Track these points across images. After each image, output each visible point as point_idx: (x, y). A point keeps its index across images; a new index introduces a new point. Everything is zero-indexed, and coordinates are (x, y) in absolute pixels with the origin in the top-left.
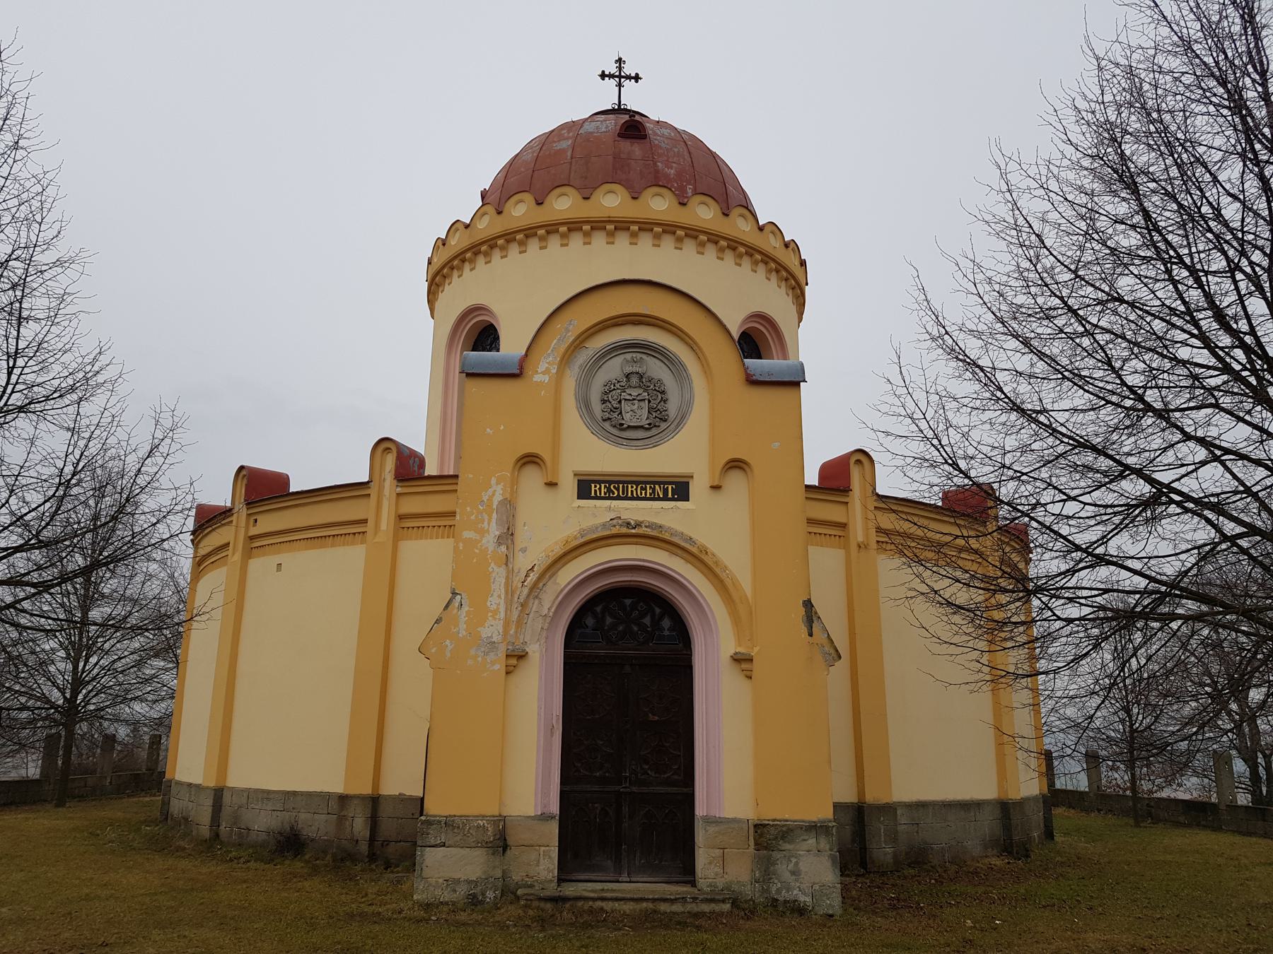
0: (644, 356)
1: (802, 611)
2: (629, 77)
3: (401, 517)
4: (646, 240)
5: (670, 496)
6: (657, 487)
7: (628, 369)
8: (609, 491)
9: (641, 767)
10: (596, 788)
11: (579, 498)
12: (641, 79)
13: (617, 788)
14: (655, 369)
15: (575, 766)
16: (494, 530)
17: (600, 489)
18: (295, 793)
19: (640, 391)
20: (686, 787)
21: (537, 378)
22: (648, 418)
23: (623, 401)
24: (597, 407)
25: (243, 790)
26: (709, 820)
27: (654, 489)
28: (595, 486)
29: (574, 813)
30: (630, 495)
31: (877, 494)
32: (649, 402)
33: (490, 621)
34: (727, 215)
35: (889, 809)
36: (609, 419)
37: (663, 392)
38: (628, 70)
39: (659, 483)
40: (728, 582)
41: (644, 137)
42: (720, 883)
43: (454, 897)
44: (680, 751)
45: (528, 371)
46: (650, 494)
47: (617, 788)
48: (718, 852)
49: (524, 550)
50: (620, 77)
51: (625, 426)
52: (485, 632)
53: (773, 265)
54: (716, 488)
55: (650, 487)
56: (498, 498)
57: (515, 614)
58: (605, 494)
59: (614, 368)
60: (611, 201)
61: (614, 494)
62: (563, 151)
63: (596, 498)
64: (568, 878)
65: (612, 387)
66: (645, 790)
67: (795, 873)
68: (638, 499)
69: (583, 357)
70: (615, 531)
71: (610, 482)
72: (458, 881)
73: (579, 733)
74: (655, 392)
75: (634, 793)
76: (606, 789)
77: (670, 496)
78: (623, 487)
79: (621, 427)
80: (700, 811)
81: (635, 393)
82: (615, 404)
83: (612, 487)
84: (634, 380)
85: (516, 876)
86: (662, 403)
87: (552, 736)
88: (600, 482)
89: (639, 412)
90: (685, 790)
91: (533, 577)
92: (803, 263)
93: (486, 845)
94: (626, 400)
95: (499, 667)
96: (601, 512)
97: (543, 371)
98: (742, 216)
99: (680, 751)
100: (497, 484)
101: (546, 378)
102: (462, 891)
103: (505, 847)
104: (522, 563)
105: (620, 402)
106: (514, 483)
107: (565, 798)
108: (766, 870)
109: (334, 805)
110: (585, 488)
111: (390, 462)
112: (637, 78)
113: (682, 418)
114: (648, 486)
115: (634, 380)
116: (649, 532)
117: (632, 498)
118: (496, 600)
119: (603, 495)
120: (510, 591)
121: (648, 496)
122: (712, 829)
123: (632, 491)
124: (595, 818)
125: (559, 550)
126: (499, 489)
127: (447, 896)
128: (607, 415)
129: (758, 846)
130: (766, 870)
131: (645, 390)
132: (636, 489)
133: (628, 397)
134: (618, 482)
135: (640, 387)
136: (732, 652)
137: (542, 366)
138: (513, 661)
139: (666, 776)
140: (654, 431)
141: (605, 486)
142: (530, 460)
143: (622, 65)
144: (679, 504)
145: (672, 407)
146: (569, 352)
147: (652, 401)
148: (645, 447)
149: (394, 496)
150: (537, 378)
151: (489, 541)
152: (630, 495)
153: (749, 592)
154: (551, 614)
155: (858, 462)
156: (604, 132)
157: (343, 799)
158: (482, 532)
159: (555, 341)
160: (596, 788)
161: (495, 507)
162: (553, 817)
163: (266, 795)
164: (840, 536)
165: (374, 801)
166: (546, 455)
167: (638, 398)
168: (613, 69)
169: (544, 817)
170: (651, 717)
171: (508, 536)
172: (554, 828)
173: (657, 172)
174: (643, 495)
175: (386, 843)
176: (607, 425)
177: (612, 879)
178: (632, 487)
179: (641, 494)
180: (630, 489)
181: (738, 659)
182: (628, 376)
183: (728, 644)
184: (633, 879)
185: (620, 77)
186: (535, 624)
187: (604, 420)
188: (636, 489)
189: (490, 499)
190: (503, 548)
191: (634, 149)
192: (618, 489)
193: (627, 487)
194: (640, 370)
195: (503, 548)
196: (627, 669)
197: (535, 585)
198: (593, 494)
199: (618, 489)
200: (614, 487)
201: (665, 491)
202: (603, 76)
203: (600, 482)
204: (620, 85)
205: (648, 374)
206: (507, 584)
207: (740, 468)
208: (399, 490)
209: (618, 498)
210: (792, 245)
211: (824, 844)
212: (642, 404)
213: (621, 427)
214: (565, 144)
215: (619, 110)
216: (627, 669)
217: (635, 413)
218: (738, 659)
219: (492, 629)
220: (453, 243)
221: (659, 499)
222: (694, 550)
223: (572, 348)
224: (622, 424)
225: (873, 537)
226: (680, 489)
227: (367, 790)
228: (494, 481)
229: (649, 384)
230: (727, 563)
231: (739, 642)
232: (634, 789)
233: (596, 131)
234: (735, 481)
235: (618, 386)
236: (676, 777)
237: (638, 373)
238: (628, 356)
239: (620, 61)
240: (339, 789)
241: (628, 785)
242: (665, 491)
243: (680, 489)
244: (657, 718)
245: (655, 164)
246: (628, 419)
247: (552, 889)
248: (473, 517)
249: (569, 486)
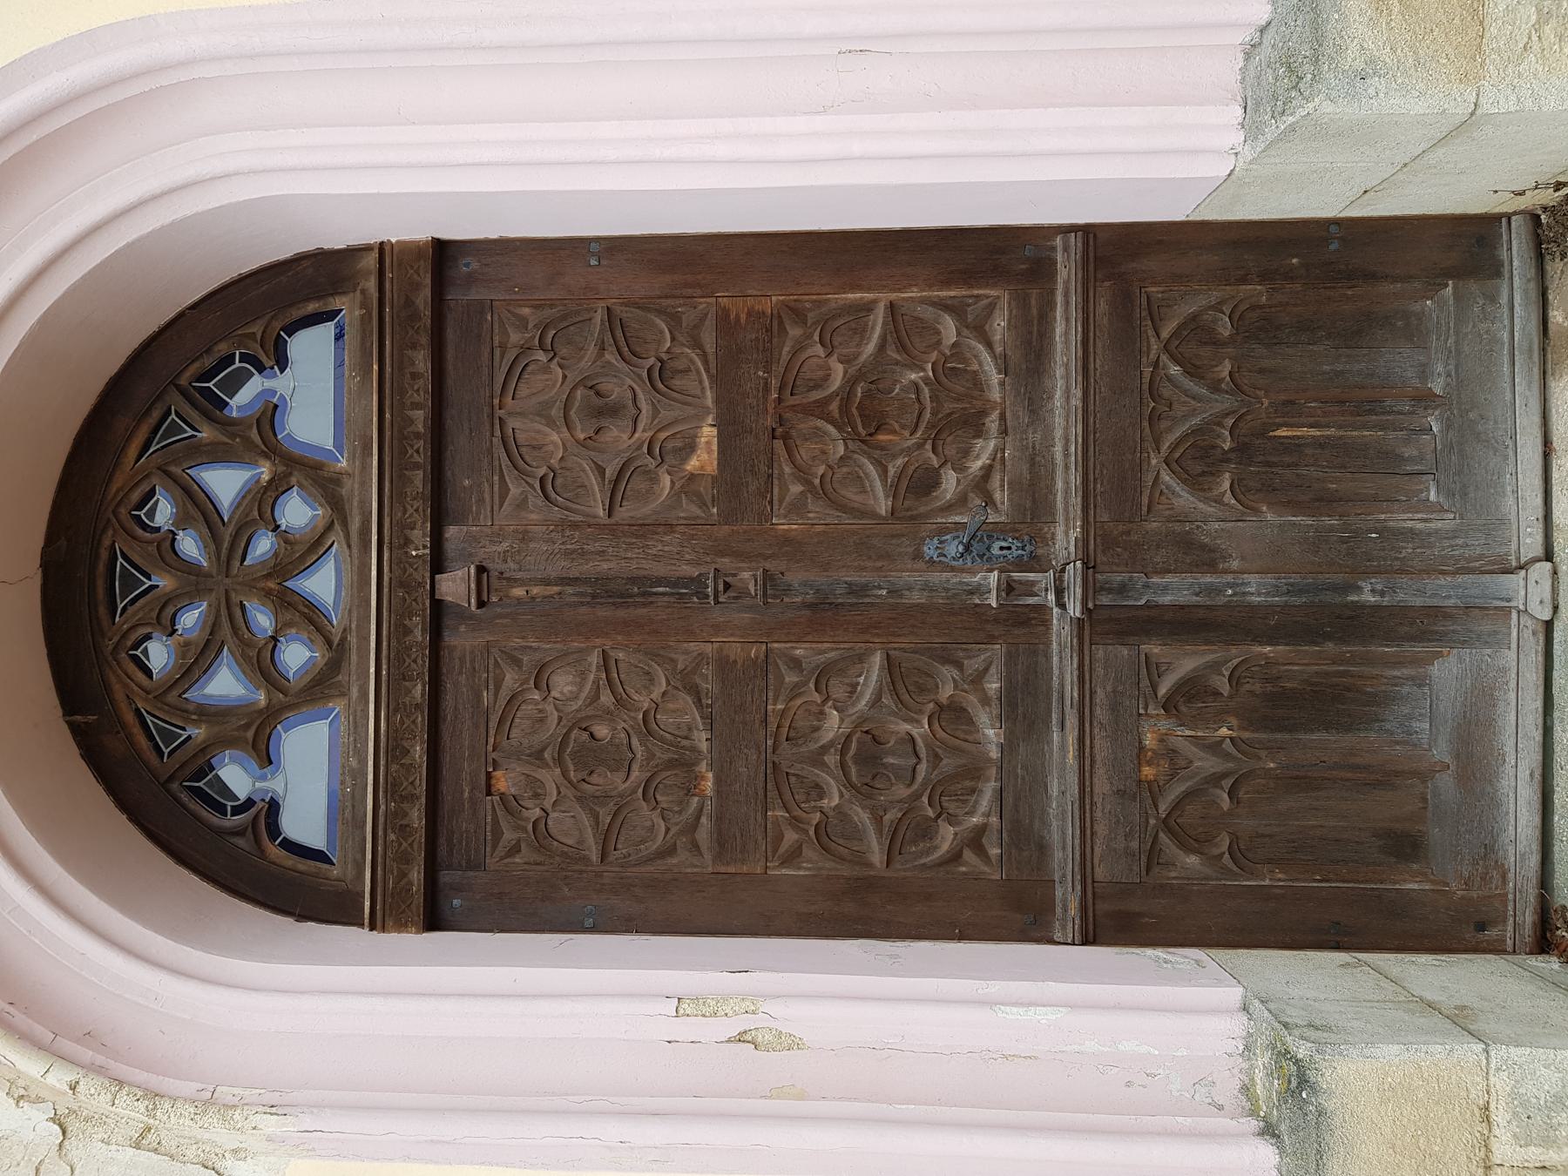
9: (949, 508)
10: (1062, 743)
13: (1060, 631)
15: (955, 857)
20: (1052, 275)
29: (1192, 860)
44: (868, 308)
47: (1060, 631)
64: (1532, 893)
66: (1066, 484)
73: (791, 836)
75: (1084, 542)
76: (1071, 692)
87: (794, 1044)
90: (1066, 271)
99: (868, 308)
124: (1215, 747)
139: (995, 377)
154: (59, 1078)
160: (1062, 743)
170: (704, 458)
177: (1534, 658)
184: (1532, 543)
196: (455, 586)
216: (455, 586)
232: (1065, 539)
236: (999, 325)
241: (1045, 579)
244: (708, 433)
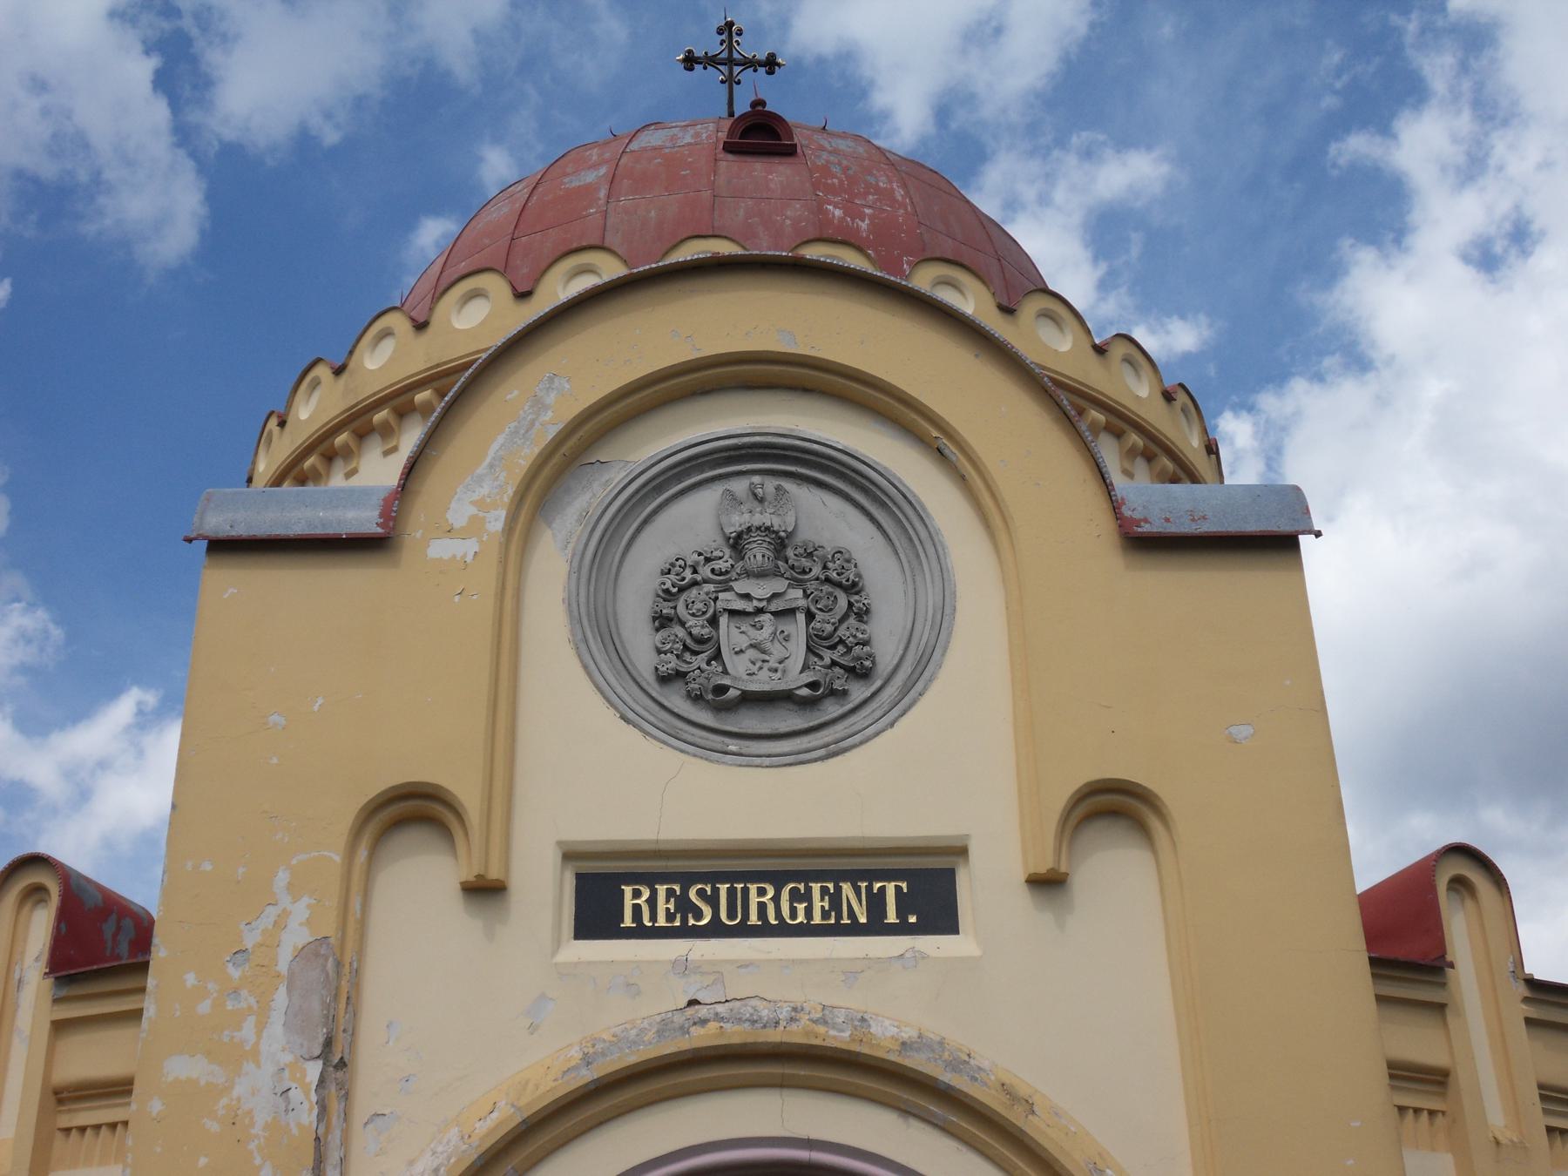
0: (788, 485)
5: (892, 918)
6: (846, 888)
7: (737, 521)
8: (684, 906)
12: (779, 65)
17: (652, 902)
19: (779, 585)
21: (441, 549)
22: (805, 667)
23: (724, 620)
24: (642, 644)
27: (836, 900)
28: (637, 894)
30: (754, 919)
31: (1532, 983)
32: (810, 616)
36: (680, 675)
37: (853, 588)
39: (854, 876)
41: (790, 151)
45: (415, 528)
46: (825, 915)
50: (730, 62)
51: (732, 693)
53: (1135, 439)
55: (824, 891)
56: (296, 936)
58: (670, 917)
61: (699, 915)
62: (588, 191)
63: (640, 932)
65: (688, 574)
68: (783, 930)
71: (687, 879)
74: (827, 588)
77: (892, 918)
78: (732, 893)
79: (719, 699)
81: (761, 590)
82: (699, 627)
83: (692, 895)
84: (758, 553)
86: (852, 621)
88: (651, 879)
89: (777, 651)
94: (733, 613)
98: (1046, 315)
100: (294, 890)
101: (469, 547)
105: (714, 622)
114: (816, 888)
115: (758, 553)
117: (765, 930)
119: (662, 921)
121: (817, 919)
123: (762, 907)
126: (300, 910)
128: (672, 663)
131: (797, 583)
132: (776, 899)
133: (739, 605)
134: (715, 878)
135: (776, 573)
137: (460, 512)
140: (832, 709)
141: (670, 893)
143: (735, 38)
146: (547, 471)
147: (820, 616)
148: (800, 759)
149: (46, 1027)
152: (754, 919)
155: (1459, 883)
156: (689, 144)
158: (235, 1057)
159: (501, 439)
161: (283, 967)
164: (1432, 1113)
166: (467, 793)
167: (774, 607)
168: (714, 46)
174: (801, 918)
178: (762, 892)
179: (794, 915)
180: (754, 900)
182: (737, 544)
185: (730, 62)
187: (664, 679)
188: (776, 899)
189: (270, 943)
192: (713, 901)
193: (746, 891)
194: (776, 522)
198: (628, 922)
199: (713, 901)
200: (701, 893)
201: (876, 904)
202: (690, 61)
205: (805, 535)
207: (1113, 813)
209: (716, 930)
210: (1181, 398)
212: (787, 626)
213: (719, 699)
221: (855, 929)
223: (557, 459)
224: (721, 690)
225: (1537, 1119)
228: (282, 878)
229: (805, 563)
233: (668, 144)
235: (705, 571)
237: (768, 529)
238: (740, 486)
242: (876, 904)
246: (742, 672)
248: (204, 1007)
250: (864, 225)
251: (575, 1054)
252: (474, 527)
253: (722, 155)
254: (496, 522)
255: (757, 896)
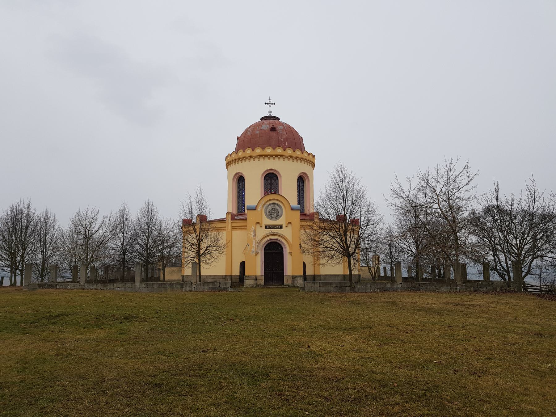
1: (299, 246)
2: (272, 104)
3: (232, 227)
4: (276, 159)
7: (273, 208)
8: (270, 227)
11: (266, 228)
14: (277, 207)
16: (253, 234)
18: (216, 275)
21: (258, 210)
24: (268, 214)
25: (205, 275)
26: (285, 275)
33: (253, 248)
34: (294, 152)
35: (320, 276)
38: (271, 102)
40: (288, 241)
42: (287, 284)
43: (250, 286)
45: (257, 209)
48: (287, 280)
49: (257, 237)
50: (270, 104)
52: (252, 250)
54: (287, 227)
57: (257, 247)
59: (270, 207)
60: (269, 150)
62: (257, 134)
66: (276, 272)
67: (297, 282)
69: (265, 206)
70: (271, 234)
71: (270, 226)
72: (250, 284)
80: (284, 274)
84: (274, 209)
85: (258, 284)
91: (259, 241)
92: (314, 157)
93: (254, 279)
95: (255, 255)
96: (269, 231)
97: (259, 209)
101: (260, 210)
102: (251, 285)
103: (257, 280)
104: (257, 239)
106: (255, 227)
107: (265, 273)
108: (293, 282)
109: (224, 277)
110: (266, 227)
111: (230, 216)
112: (274, 104)
113: (281, 215)
115: (274, 209)
116: (276, 234)
118: (254, 245)
120: (256, 244)
122: (286, 277)
125: (263, 237)
127: (249, 286)
129: (292, 279)
130: (293, 282)
136: (289, 251)
138: (256, 254)
140: (277, 217)
142: (258, 223)
144: (281, 229)
145: (280, 214)
150: (258, 210)
151: (252, 236)
153: (291, 242)
157: (226, 276)
158: (251, 235)
162: (263, 276)
163: (210, 276)
165: (231, 276)
166: (260, 222)
168: (269, 102)
169: (262, 276)
171: (255, 235)
172: (263, 277)
173: (279, 140)
175: (233, 283)
176: (269, 217)
181: (290, 253)
182: (273, 209)
183: (288, 251)
186: (259, 248)
190: (254, 237)
191: (273, 134)
194: (274, 208)
195: (254, 237)
197: (259, 242)
202: (266, 104)
203: (269, 226)
204: (270, 106)
206: (255, 242)
208: (232, 222)
209: (272, 228)
211: (301, 278)
214: (258, 132)
215: (270, 117)
217: (274, 215)
218: (290, 253)
219: (253, 249)
220: (233, 157)
222: (283, 236)
226: (281, 227)
227: (230, 274)
230: (289, 239)
231: (290, 250)
234: (290, 225)
238: (273, 205)
239: (270, 99)
240: (225, 274)
243: (281, 227)
245: (278, 138)
246: (273, 216)
247: (264, 285)
249: (264, 227)
250: (282, 139)
251: (265, 234)
252: (260, 209)
253: (270, 131)
254: (261, 208)
255: (273, 227)
